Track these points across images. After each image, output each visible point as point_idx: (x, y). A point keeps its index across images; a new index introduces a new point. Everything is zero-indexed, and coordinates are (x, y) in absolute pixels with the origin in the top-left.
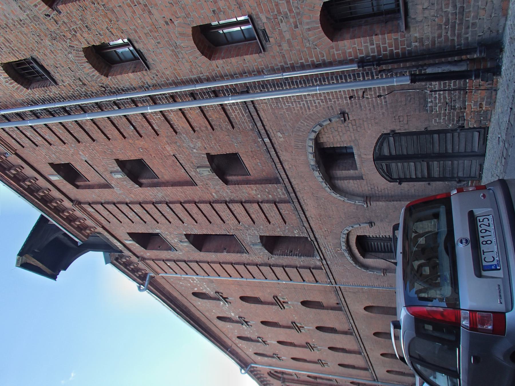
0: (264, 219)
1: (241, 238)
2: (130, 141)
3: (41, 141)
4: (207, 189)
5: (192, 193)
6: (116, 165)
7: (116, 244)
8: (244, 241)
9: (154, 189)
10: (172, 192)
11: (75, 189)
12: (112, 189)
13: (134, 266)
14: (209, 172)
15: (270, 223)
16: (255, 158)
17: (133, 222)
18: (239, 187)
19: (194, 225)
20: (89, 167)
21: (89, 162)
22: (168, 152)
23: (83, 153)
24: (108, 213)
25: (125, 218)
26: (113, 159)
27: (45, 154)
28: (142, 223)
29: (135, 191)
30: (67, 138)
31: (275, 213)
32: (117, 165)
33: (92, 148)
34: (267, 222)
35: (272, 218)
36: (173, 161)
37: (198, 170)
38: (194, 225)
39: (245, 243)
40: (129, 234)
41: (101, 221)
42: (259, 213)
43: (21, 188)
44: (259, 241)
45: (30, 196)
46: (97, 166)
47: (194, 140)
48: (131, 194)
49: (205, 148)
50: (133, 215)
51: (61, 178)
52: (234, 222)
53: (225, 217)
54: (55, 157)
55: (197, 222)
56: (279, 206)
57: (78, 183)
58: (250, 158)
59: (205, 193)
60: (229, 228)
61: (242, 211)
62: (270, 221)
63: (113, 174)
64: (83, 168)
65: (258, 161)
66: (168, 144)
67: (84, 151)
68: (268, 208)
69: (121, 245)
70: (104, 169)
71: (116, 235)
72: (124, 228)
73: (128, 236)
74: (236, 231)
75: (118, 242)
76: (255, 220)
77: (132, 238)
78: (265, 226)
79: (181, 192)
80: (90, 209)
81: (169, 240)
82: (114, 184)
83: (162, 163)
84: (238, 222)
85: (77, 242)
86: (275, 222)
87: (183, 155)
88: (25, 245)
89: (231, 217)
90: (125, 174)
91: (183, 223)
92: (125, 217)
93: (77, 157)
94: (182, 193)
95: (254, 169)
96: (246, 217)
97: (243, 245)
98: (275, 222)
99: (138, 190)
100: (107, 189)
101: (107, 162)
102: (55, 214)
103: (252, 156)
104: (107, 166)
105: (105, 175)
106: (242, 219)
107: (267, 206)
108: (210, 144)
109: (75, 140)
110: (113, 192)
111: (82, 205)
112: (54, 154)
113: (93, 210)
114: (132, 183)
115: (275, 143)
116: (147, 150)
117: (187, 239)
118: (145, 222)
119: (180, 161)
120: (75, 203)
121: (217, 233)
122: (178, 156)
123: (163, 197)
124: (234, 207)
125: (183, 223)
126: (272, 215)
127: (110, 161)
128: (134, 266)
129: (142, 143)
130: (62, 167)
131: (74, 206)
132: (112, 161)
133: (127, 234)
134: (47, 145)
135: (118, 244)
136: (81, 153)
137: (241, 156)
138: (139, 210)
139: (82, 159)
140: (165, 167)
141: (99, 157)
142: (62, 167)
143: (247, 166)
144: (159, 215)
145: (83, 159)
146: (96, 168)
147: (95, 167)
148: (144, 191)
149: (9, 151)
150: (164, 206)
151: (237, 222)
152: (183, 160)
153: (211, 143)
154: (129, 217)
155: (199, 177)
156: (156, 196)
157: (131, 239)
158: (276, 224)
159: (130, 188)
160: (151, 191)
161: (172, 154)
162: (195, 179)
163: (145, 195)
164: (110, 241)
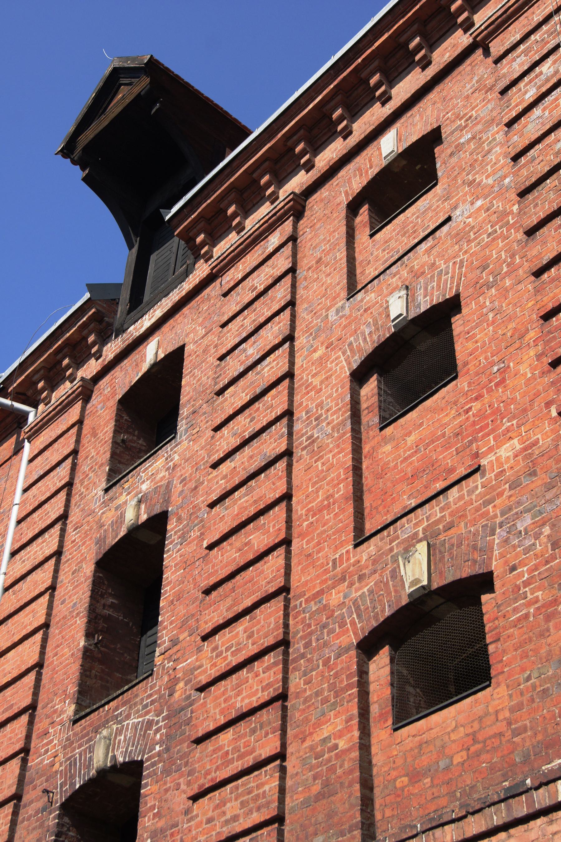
0: (213, 774)
1: (137, 696)
2: (532, 335)
3: (523, 100)
4: (343, 579)
5: (325, 531)
6: (437, 298)
7: (146, 317)
8: (124, 704)
9: (345, 412)
10: (332, 465)
11: (344, 200)
12: (344, 294)
13: (94, 344)
14: (412, 584)
15: (195, 798)
16: (472, 749)
17: (222, 358)
18: (349, 687)
19: (201, 537)
20: (423, 231)
21: (445, 229)
22: (491, 450)
23: (479, 209)
24: (261, 288)
25: (240, 334)
26: (457, 290)
27: (470, 117)
28: (216, 384)
29: (339, 357)
30: (537, 161)
31: (235, 818)
32: (434, 302)
33: (499, 232)
34: (200, 786)
35: (217, 807)
36: (452, 470)
37: (422, 547)
38: (201, 537)
39: (117, 709)
40: (181, 350)
41: (232, 270)
42: (240, 758)
43: (362, 61)
44: (121, 759)
45: (335, 83)
46: (432, 247)
47: (547, 530)
48: (327, 348)
49: (513, 568)
50: (247, 357)
51: (384, 163)
52: (205, 671)
53: (229, 640)
54: (462, 140)
55: (211, 547)
56: (265, 831)
57: (364, 210)
58: (470, 731)
59: (326, 571)
60: (179, 654)
61: (249, 696)
62: (204, 801)
63: (403, 292)
64: (418, 217)
65: (457, 759)
66: (525, 449)
67: (488, 210)
68: (261, 791)
69: (144, 329)
70: (418, 269)
71: (178, 317)
72: (203, 337)
73: (170, 349)
74: (166, 679)
75: (153, 320)
76: (209, 746)
77: (162, 360)
78: (181, 780)
79: (332, 496)
80: (274, 240)
81: (147, 464)
82: (362, 300)
83: (444, 435)
84: (204, 682)
85: (170, 208)
86: (197, 816)
87: (481, 496)
88: (176, 80)
89: (226, 658)
90: (401, 326)
91: (212, 505)
92: (244, 335)
93: (465, 195)
94: (327, 498)
95: (420, 745)
96: (222, 712)
97: (108, 703)
98: (197, 816)
99: (342, 368)
100: (345, 281)
101: (447, 273)
102: (270, 148)
103: (480, 738)
104: (432, 277)
105: (398, 273)
106: (216, 698)
107: (267, 788)
108: (530, 584)
109: (528, 184)
110: (335, 298)
111: (291, 218)
112: (474, 138)
113: (271, 249)
114: (369, 348)
115: (551, 822)
116: (497, 385)
117: (148, 520)
118: (220, 392)
119: (455, 489)
120: (300, 200)
121: (164, 615)
122: (478, 480)
123: (313, 442)
124: (268, 668)
125: (212, 505)
126: (228, 805)
127: (452, 283)
128: (94, 344)
129: (524, 369)
130: (418, 167)
131: (291, 196)
132: (451, 288)
133: (182, 343)
134: (506, 114)
135: (147, 322)
136: (479, 203)
137: (480, 694)
138: (269, 371)
139: (456, 208)
140: (428, 445)
141: (466, 252)
142: (418, 167)
143: (434, 718)
144: (244, 432)
145: (458, 212)
146: (424, 246)
147: (429, 245)
148: (335, 384)
149: (486, 28)
150: (281, 443)
151: (204, 679)
152: (461, 498)
153: (539, 589)
154: (244, 345)
155: (391, 550)
156: (316, 419)
157: (161, 355)
158: (189, 821)
159: (350, 344)
160: (337, 405)
161: (484, 462)
162: (382, 539)
163: (321, 389)
164: (160, 300)
